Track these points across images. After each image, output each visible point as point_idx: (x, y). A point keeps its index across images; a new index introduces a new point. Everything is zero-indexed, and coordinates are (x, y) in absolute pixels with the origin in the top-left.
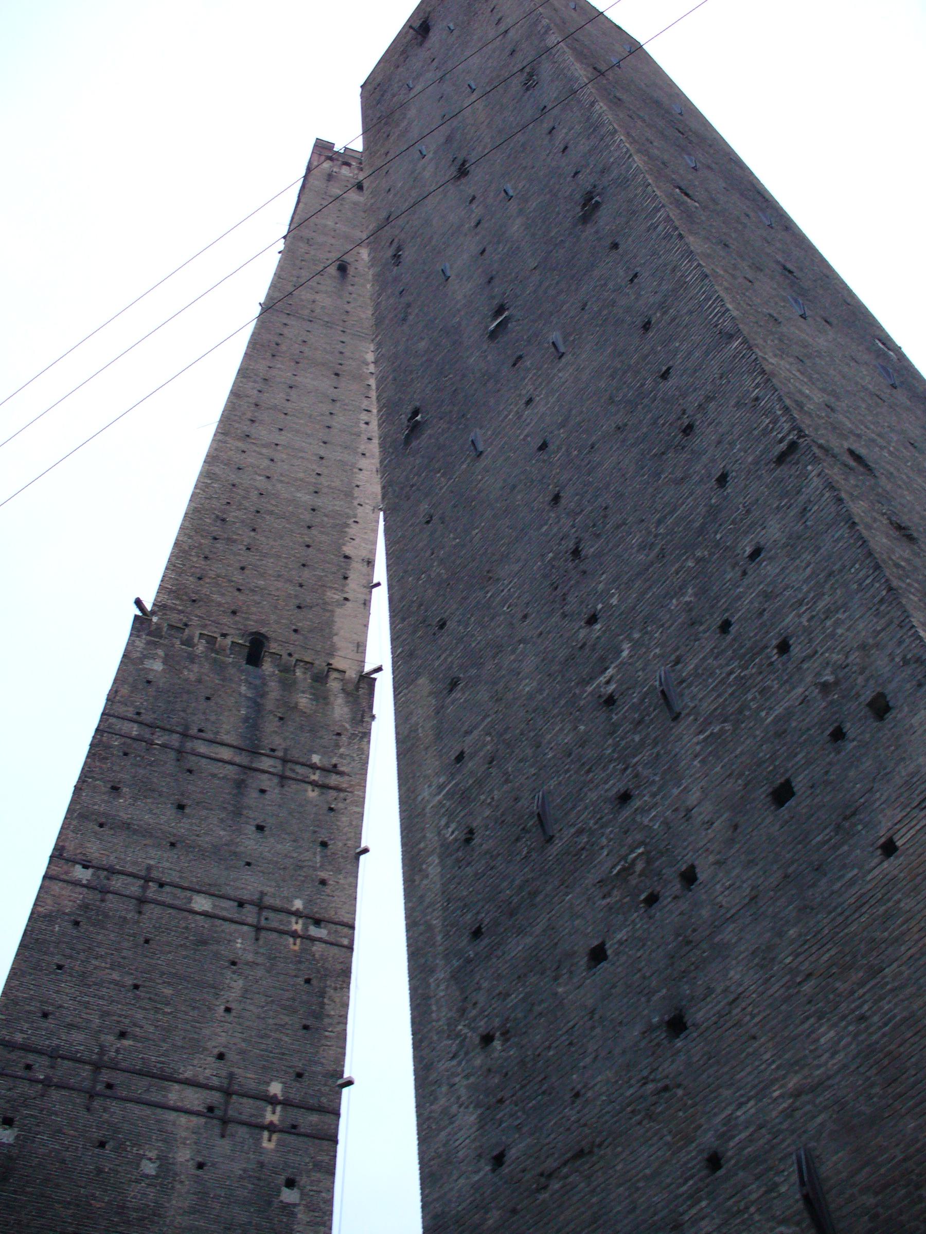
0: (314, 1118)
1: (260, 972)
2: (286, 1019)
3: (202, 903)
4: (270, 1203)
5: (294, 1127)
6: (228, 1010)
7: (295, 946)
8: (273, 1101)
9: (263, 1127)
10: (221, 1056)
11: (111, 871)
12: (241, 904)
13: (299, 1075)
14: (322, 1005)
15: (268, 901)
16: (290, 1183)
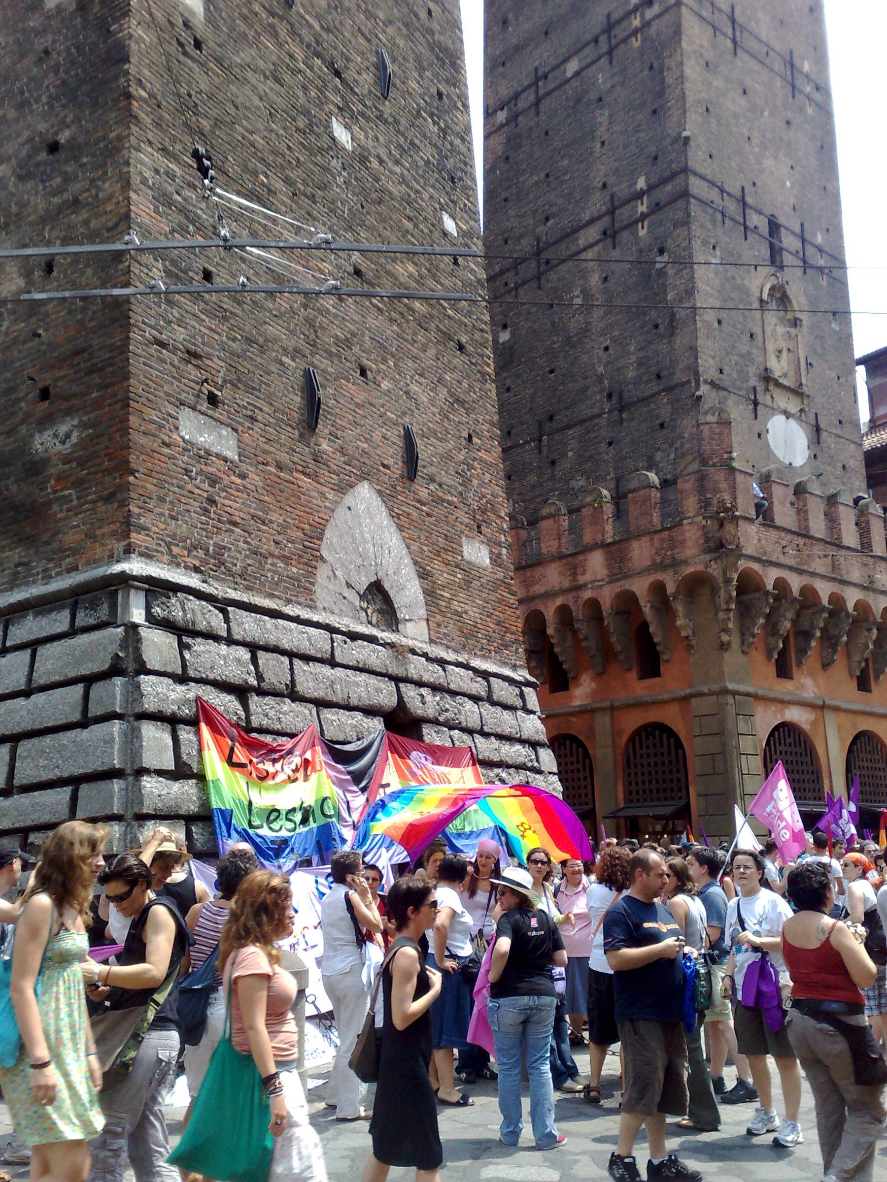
0: (669, 187)
1: (619, 89)
2: (640, 117)
3: (572, 67)
4: (650, 276)
5: (657, 205)
6: (603, 143)
7: (636, 43)
8: (640, 195)
9: (636, 222)
10: (604, 186)
11: (516, 96)
12: (596, 40)
13: (656, 158)
14: (663, 81)
15: (615, 16)
16: (661, 251)
